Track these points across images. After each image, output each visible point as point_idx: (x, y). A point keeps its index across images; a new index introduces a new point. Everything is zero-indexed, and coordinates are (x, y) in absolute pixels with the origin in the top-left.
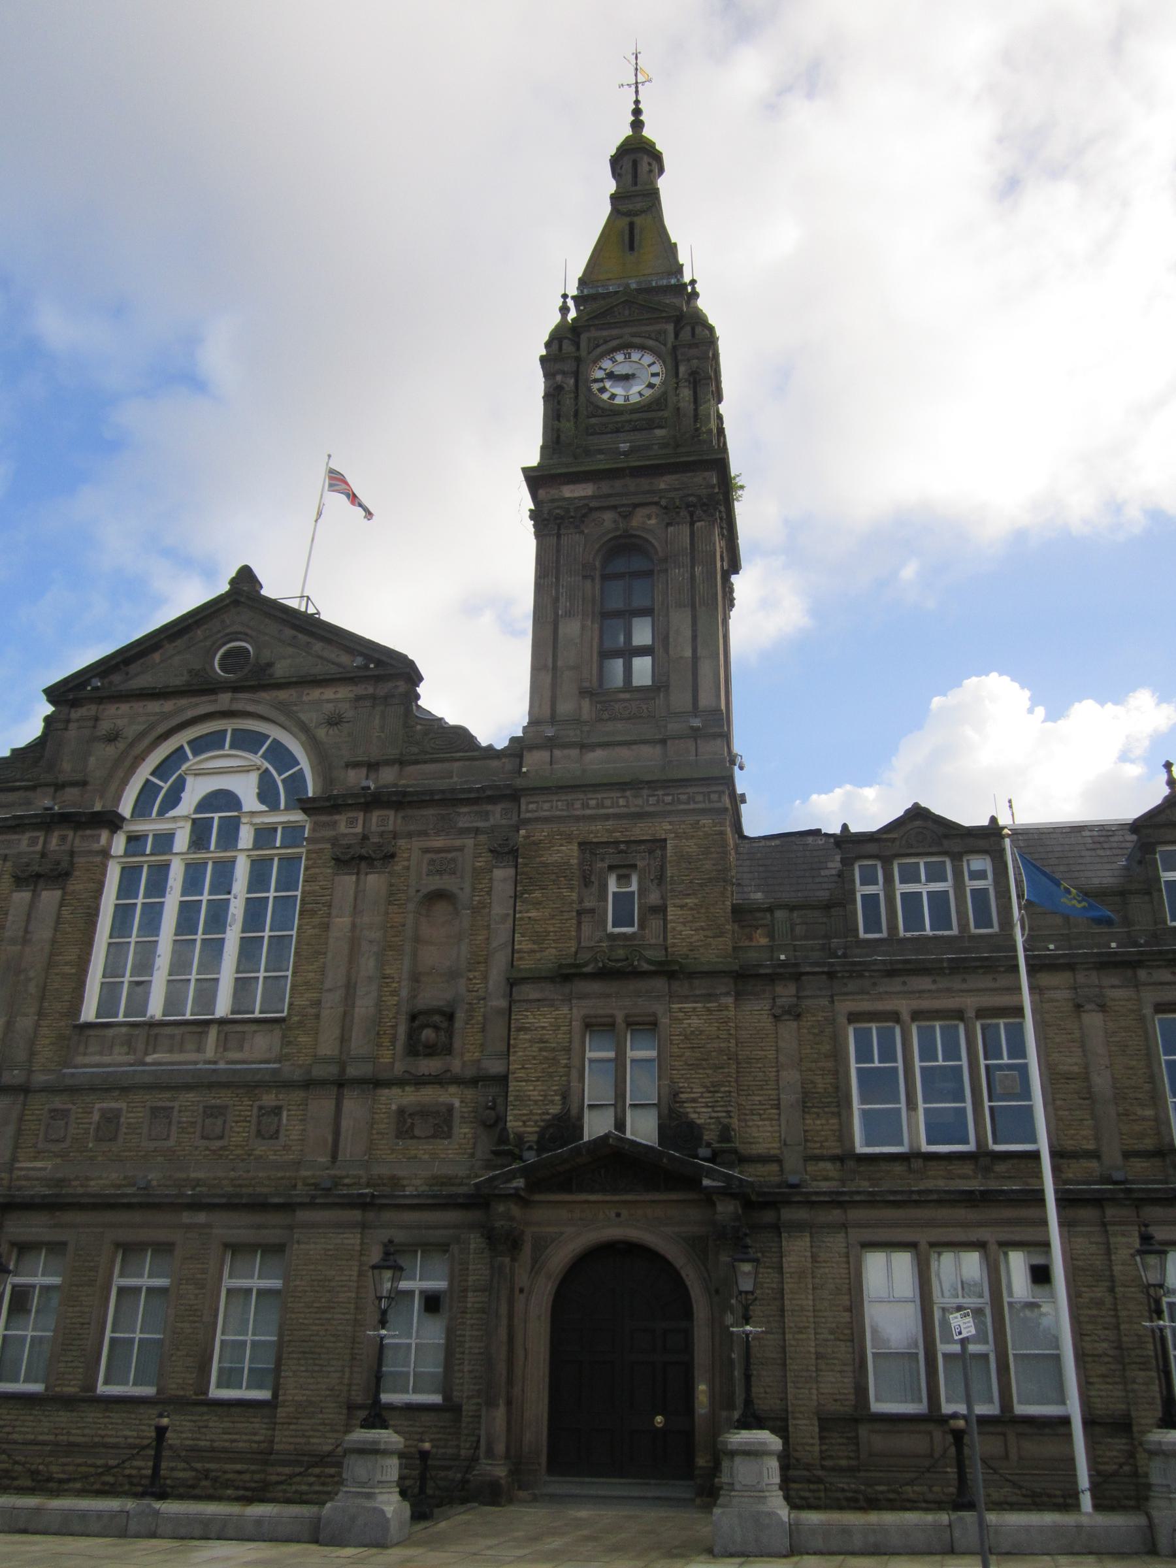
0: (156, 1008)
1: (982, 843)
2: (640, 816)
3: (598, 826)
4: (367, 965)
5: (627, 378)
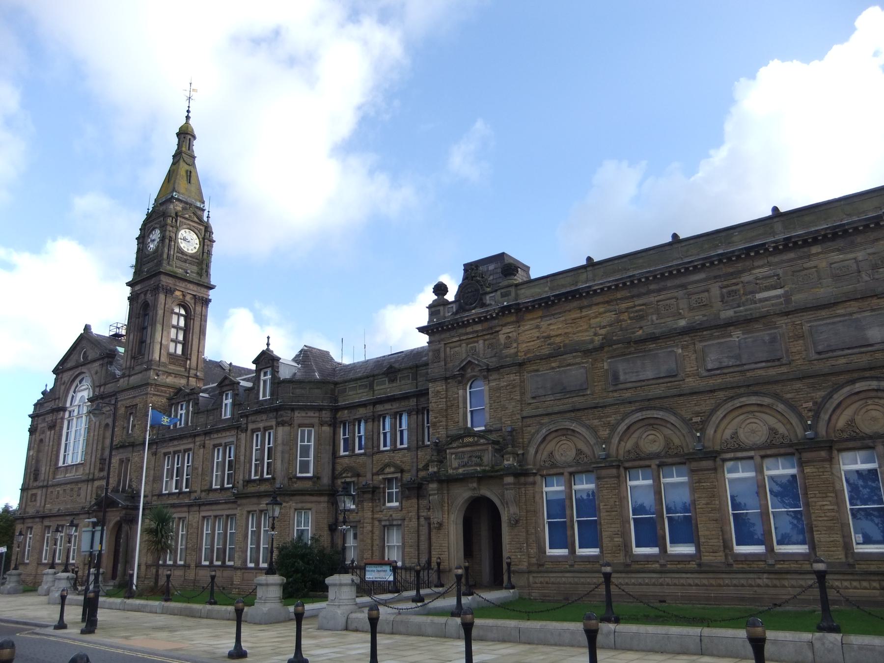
0: (69, 462)
1: (192, 397)
2: (134, 397)
3: (128, 401)
4: (95, 446)
5: (154, 240)
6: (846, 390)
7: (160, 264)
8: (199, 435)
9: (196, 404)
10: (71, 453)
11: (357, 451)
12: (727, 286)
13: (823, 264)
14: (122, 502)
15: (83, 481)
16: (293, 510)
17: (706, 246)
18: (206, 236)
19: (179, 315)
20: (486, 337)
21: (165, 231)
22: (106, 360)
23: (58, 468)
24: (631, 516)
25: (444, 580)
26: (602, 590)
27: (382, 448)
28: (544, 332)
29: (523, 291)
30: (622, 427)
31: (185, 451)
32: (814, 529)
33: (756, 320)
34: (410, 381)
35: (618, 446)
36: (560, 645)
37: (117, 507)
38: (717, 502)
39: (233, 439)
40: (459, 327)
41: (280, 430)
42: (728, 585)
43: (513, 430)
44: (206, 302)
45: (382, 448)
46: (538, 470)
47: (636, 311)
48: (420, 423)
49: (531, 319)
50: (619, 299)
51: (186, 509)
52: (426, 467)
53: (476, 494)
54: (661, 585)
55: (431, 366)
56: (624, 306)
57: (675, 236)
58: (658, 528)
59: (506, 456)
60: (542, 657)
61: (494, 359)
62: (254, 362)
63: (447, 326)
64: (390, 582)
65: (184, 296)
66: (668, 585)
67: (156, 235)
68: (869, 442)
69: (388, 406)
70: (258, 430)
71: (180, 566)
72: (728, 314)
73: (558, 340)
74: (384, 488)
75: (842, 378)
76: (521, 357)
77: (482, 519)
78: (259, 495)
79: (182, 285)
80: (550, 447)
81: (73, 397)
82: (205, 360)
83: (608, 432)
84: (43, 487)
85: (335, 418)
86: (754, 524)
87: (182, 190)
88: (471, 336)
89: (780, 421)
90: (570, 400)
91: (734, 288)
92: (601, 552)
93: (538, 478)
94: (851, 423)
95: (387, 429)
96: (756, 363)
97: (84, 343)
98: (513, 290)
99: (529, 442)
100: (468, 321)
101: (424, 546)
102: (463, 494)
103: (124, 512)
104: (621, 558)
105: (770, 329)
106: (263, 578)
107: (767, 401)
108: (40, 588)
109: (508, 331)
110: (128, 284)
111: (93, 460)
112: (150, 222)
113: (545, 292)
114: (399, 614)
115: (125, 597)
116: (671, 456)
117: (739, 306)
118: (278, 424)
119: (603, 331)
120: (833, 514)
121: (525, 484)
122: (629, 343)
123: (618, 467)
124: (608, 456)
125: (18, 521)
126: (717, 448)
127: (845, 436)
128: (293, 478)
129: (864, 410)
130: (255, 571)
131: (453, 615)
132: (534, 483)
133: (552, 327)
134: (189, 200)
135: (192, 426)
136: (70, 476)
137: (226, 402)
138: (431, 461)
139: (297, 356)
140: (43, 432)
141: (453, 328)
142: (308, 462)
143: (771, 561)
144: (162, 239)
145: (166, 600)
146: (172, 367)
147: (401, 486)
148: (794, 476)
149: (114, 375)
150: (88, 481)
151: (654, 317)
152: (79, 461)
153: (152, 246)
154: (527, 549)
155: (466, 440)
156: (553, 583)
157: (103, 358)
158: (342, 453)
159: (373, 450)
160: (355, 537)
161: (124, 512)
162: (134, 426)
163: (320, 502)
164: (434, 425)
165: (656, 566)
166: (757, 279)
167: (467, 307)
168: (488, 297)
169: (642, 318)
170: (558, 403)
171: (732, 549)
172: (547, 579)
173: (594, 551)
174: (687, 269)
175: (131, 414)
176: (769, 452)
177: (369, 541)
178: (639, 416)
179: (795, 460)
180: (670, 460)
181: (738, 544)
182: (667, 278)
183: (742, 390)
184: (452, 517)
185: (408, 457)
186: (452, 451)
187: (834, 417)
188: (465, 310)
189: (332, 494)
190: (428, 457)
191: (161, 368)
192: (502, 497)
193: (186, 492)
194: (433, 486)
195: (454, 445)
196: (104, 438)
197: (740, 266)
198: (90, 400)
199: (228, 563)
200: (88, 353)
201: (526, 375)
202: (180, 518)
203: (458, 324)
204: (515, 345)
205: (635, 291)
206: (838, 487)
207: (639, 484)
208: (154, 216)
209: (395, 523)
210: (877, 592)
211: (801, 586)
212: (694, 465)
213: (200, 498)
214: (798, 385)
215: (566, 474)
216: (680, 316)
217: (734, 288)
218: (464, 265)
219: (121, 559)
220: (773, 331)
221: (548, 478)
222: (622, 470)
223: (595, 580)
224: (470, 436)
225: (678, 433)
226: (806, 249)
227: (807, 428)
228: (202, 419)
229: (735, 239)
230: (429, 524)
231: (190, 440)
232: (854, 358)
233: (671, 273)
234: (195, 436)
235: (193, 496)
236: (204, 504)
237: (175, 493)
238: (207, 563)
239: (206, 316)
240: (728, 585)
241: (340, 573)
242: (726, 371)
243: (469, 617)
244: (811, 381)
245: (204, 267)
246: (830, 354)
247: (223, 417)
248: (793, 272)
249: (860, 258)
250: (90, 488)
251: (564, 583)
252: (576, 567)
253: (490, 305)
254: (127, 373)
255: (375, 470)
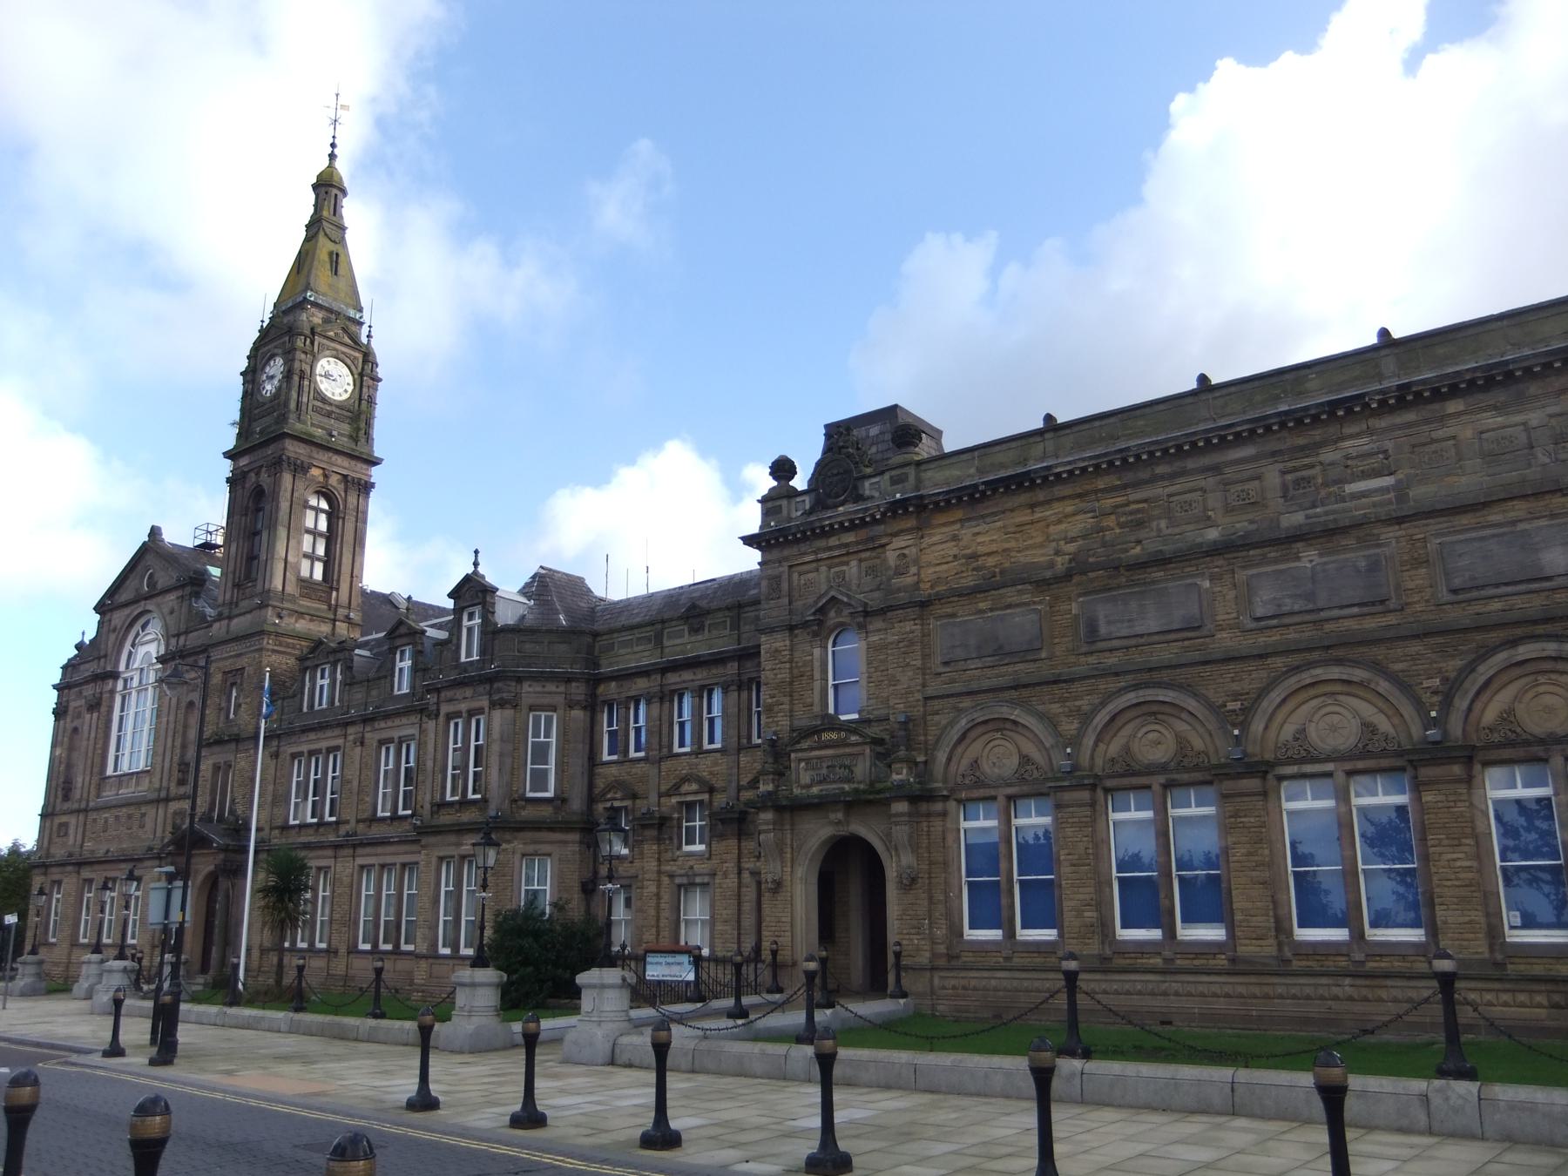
0: (125, 767)
1: (340, 656)
3: (228, 663)
5: (272, 377)
6: (1501, 658)
7: (283, 419)
8: (353, 723)
9: (348, 668)
10: (127, 752)
11: (632, 754)
12: (1295, 470)
13: (1468, 433)
14: (218, 840)
15: (151, 802)
16: (518, 856)
17: (1258, 398)
18: (365, 368)
19: (317, 510)
20: (864, 555)
21: (293, 360)
22: (188, 589)
23: (104, 778)
24: (1114, 873)
25: (784, 981)
26: (1062, 1001)
27: (677, 749)
28: (966, 547)
29: (929, 474)
30: (1102, 718)
31: (329, 750)
32: (1437, 901)
33: (1343, 530)
34: (727, 632)
35: (1094, 750)
36: (986, 1096)
37: (211, 847)
38: (1267, 852)
39: (414, 731)
40: (816, 536)
41: (497, 715)
42: (1281, 997)
43: (908, 720)
44: (365, 488)
45: (677, 749)
46: (952, 791)
47: (1131, 513)
48: (744, 705)
49: (944, 525)
50: (1102, 491)
51: (330, 852)
52: (754, 784)
53: (843, 831)
54: (1165, 994)
55: (764, 605)
56: (1108, 502)
57: (1203, 379)
58: (1162, 895)
59: (895, 766)
60: (953, 1116)
61: (876, 594)
62: (450, 595)
63: (794, 535)
64: (688, 983)
65: (326, 476)
66: (1177, 994)
67: (276, 367)
68: (1538, 750)
69: (687, 675)
70: (458, 714)
71: (321, 951)
72: (1294, 519)
73: (991, 561)
74: (680, 820)
75: (1495, 637)
76: (926, 590)
77: (850, 874)
78: (461, 830)
79: (322, 457)
80: (974, 750)
81: (130, 653)
82: (363, 592)
83: (1076, 725)
84: (78, 811)
85: (593, 695)
86: (1327, 892)
87: (323, 288)
88: (836, 553)
89: (1381, 711)
90: (1010, 669)
91: (1305, 473)
92: (1061, 935)
93: (952, 805)
94: (1508, 716)
95: (686, 716)
96: (1342, 607)
97: (149, 559)
98: (911, 471)
99: (938, 741)
100: (831, 525)
101: (748, 921)
102: (818, 832)
103: (222, 856)
104: (1094, 948)
105: (1368, 547)
106: (466, 974)
107: (1359, 674)
108: (76, 987)
109: (903, 544)
110: (228, 455)
111: (167, 765)
112: (265, 345)
113: (968, 475)
114: (705, 1037)
115: (225, 1004)
116: (1187, 770)
117: (1314, 506)
118: (493, 705)
119: (1071, 548)
120: (1470, 875)
121: (929, 815)
122: (1116, 568)
123: (1093, 787)
124: (1075, 768)
125: (36, 871)
126: (1269, 756)
127: (1496, 738)
128: (521, 800)
129: (1530, 694)
130: (451, 962)
131: (799, 1040)
132: (944, 814)
133: (980, 539)
134: (335, 306)
135: (341, 707)
136: (126, 792)
137: (402, 664)
138: (762, 773)
139: (527, 585)
140: (79, 716)
141: (805, 539)
142: (545, 772)
143: (1359, 956)
144: (288, 375)
145: (297, 1010)
146: (305, 603)
147: (710, 816)
148: (1401, 810)
149: (202, 617)
150: (158, 801)
151: (1163, 524)
152: (141, 766)
153: (268, 387)
154: (931, 928)
155: (825, 736)
156: (975, 989)
157: (183, 586)
158: (606, 757)
159: (661, 753)
160: (628, 903)
161: (222, 856)
162: (238, 706)
163: (565, 842)
164: (769, 709)
165: (1158, 961)
166: (1347, 457)
167: (830, 502)
168: (867, 484)
169: (1140, 524)
170: (989, 672)
171: (1290, 933)
172: (962, 982)
173: (1048, 934)
174: (1223, 438)
175: (233, 684)
176: (1360, 765)
177: (652, 912)
178: (1131, 698)
179: (1406, 779)
180: (1185, 777)
181: (1300, 926)
182: (1188, 454)
183: (1315, 655)
184: (800, 872)
185: (723, 765)
186: (800, 755)
187: (1478, 706)
188: (826, 508)
189: (588, 830)
190: (758, 766)
191: (286, 605)
192: (887, 838)
193: (330, 824)
194: (767, 816)
195: (805, 745)
196: (186, 726)
197: (1317, 434)
198: (160, 659)
199: (405, 947)
200: (156, 576)
201: (933, 624)
202: (319, 869)
203: (813, 530)
204: (914, 570)
205: (1129, 477)
206: (1480, 827)
207: (1129, 818)
208: (273, 331)
209: (698, 880)
210: (1542, 1012)
211: (1410, 1000)
212: (1228, 786)
213: (355, 834)
214: (1415, 647)
215: (1001, 800)
216: (1208, 522)
217: (1305, 473)
218: (826, 426)
219: (217, 936)
220: (1372, 551)
221: (969, 805)
222: (1100, 793)
223: (1047, 985)
224: (832, 729)
225: (1201, 730)
226: (1436, 406)
227: (1429, 723)
228: (358, 695)
229: (1310, 385)
230: (759, 883)
231: (337, 732)
232: (1518, 602)
233: (1194, 444)
234: (346, 724)
235: (343, 829)
236: (362, 844)
237: (311, 825)
238: (368, 947)
239: (365, 513)
240: (1281, 997)
241: (601, 966)
242: (1286, 620)
243: (829, 1043)
244: (1440, 640)
245: (363, 425)
246: (1475, 594)
247: (396, 692)
248: (1414, 446)
249: (1534, 423)
250: (161, 812)
251: (996, 989)
252: (1017, 961)
253: (871, 498)
254: (226, 612)
255: (664, 788)
